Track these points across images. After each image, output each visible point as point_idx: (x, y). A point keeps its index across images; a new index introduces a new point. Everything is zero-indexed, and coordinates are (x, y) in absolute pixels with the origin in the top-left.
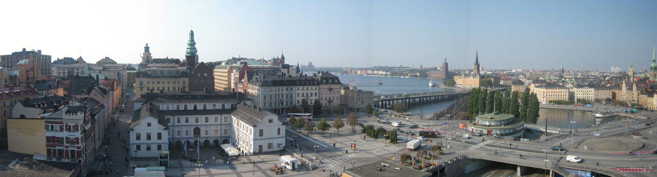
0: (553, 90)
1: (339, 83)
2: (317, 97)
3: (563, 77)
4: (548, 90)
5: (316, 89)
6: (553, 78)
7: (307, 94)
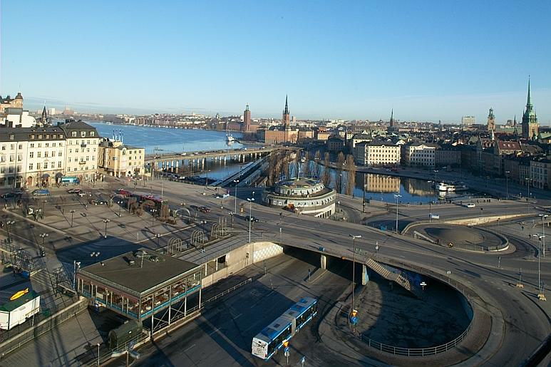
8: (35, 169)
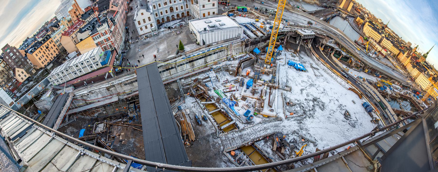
0: (375, 32)
3: (384, 29)
4: (372, 30)
6: (380, 26)
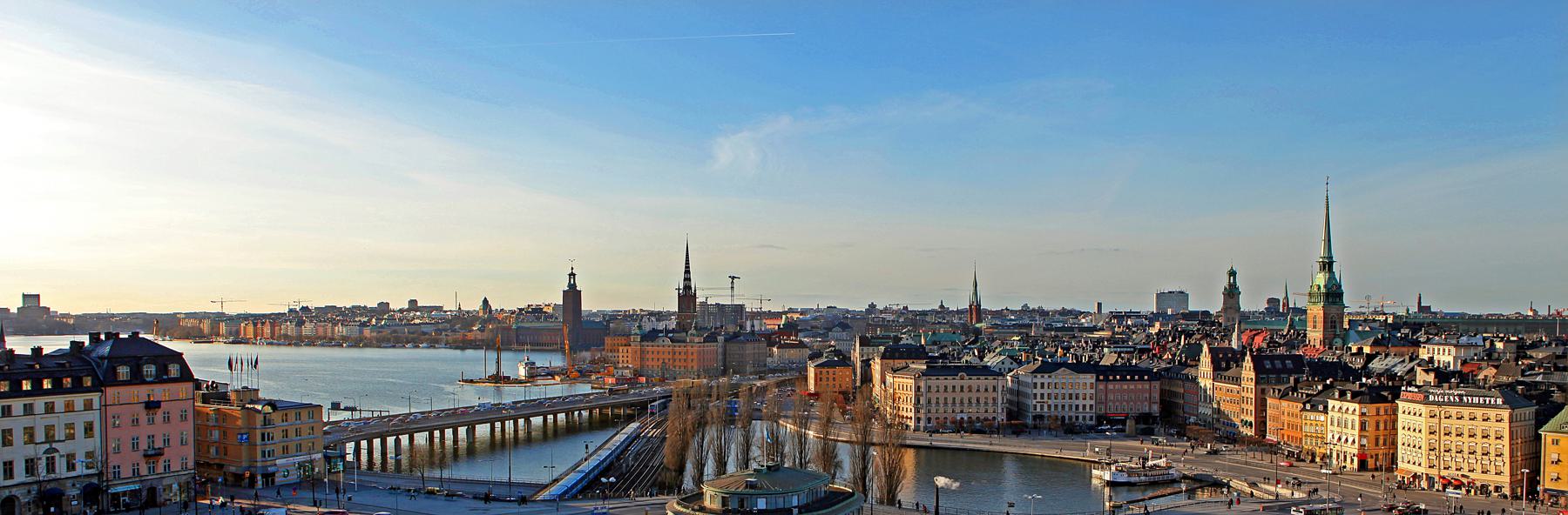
1: (186, 375)
2: (94, 443)
5: (88, 406)
7: (49, 429)
8: (20, 475)
